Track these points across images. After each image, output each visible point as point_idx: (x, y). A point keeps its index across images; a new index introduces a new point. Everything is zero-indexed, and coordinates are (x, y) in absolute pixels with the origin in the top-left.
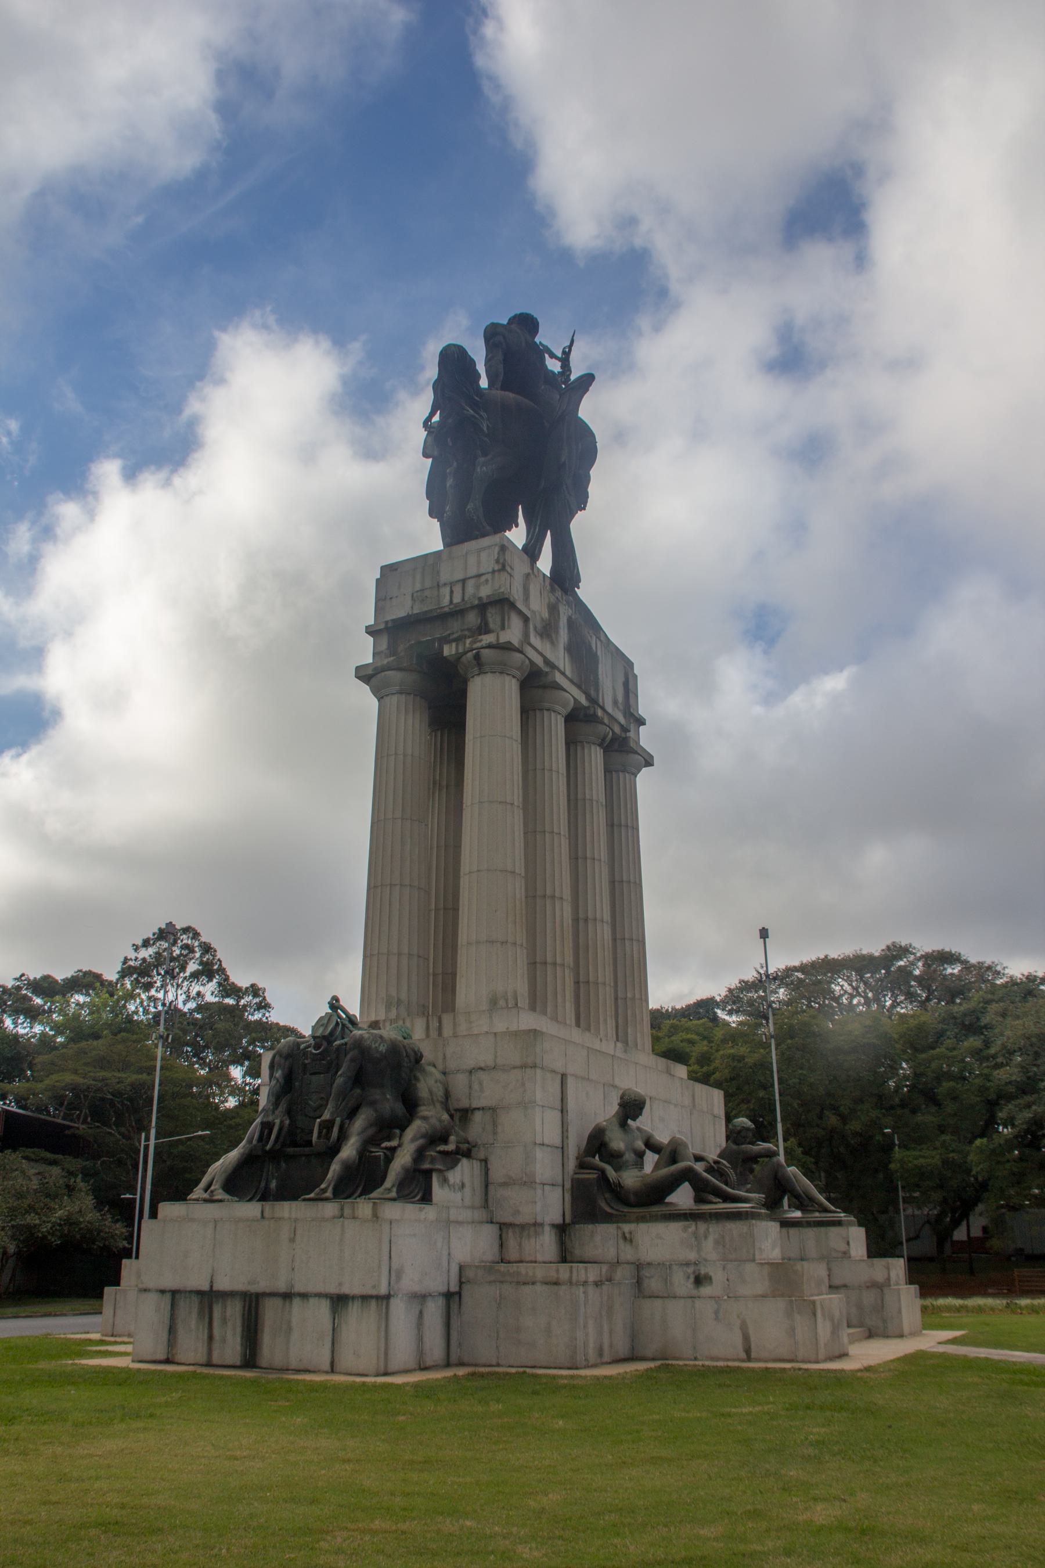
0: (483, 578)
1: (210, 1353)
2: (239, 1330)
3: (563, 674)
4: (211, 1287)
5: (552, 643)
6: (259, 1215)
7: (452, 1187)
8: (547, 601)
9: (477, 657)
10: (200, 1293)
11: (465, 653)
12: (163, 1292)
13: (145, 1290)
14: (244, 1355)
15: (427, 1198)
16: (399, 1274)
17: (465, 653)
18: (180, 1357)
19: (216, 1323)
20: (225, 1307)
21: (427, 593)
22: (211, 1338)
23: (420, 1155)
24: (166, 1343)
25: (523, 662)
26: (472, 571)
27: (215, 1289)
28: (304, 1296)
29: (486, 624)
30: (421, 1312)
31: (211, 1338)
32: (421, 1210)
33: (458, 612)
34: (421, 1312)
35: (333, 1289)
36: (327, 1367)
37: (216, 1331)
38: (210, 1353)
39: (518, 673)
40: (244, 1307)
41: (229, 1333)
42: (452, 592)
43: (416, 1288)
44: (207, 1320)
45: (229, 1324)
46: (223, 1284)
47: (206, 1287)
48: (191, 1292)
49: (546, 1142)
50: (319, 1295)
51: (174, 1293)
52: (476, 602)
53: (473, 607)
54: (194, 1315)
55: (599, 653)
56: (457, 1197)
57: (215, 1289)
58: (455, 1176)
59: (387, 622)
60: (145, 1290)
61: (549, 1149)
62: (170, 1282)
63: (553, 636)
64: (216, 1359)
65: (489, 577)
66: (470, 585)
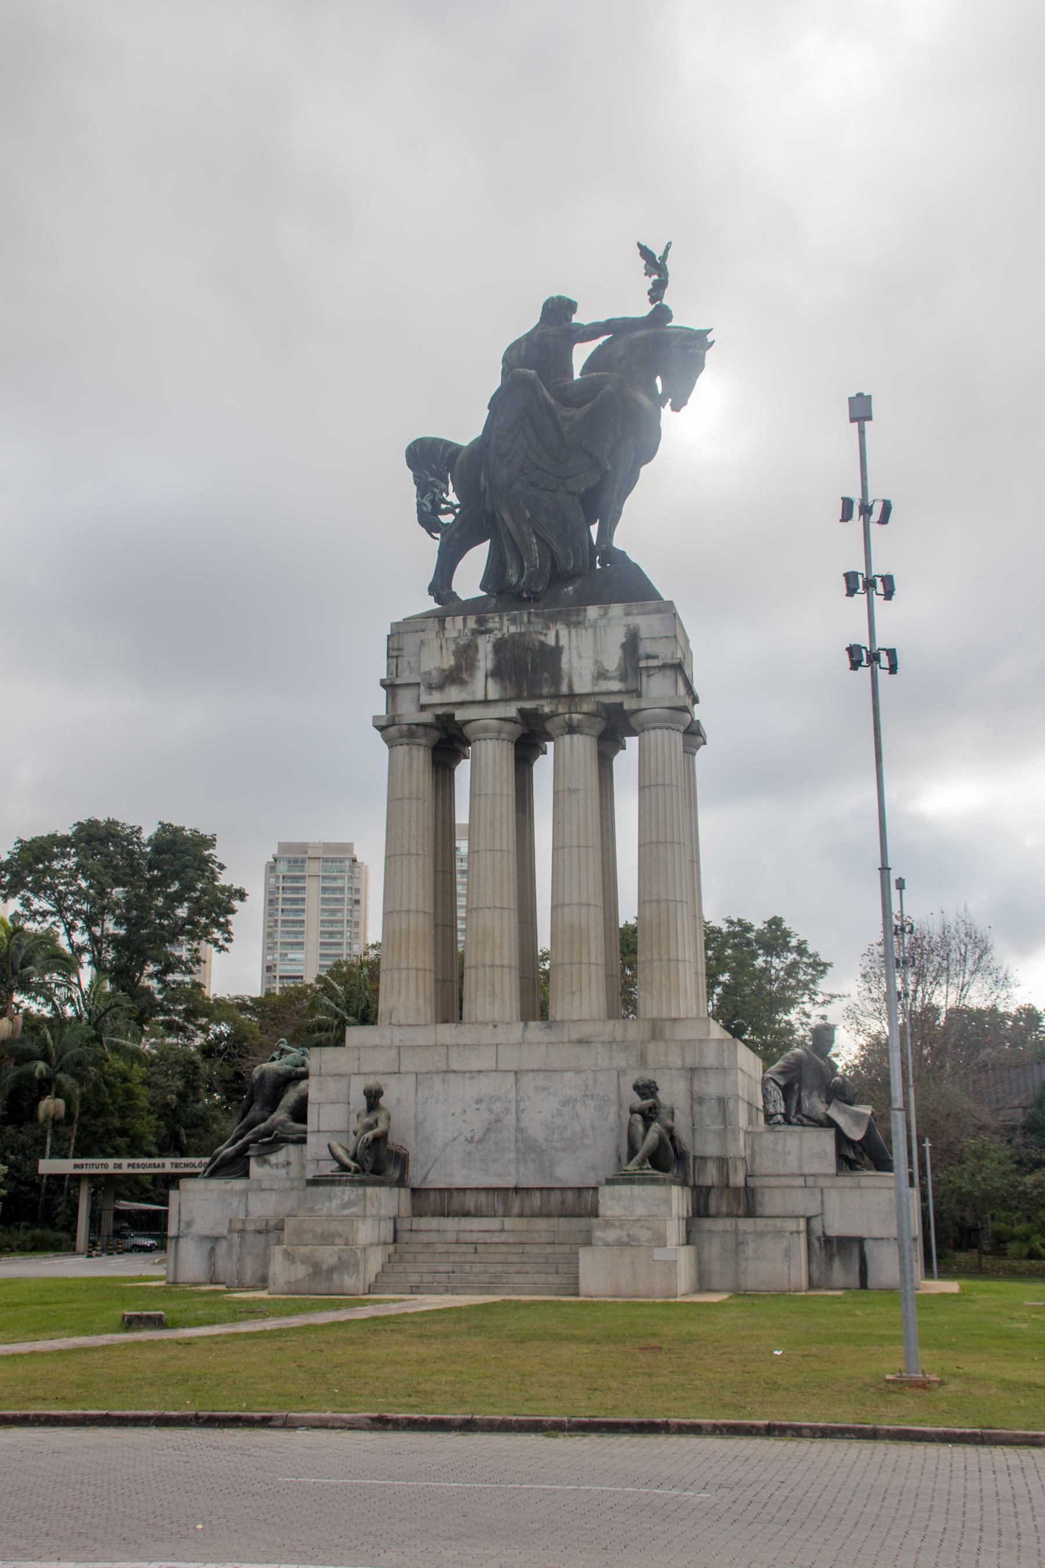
3: (486, 702)
5: (461, 682)
7: (277, 1166)
8: (452, 647)
15: (246, 1174)
16: (189, 1224)
23: (246, 1147)
25: (400, 731)
30: (213, 1249)
32: (227, 1183)
34: (213, 1249)
39: (405, 740)
43: (207, 1232)
49: (322, 1128)
55: (563, 642)
56: (283, 1172)
58: (278, 1158)
61: (327, 1134)
63: (465, 676)
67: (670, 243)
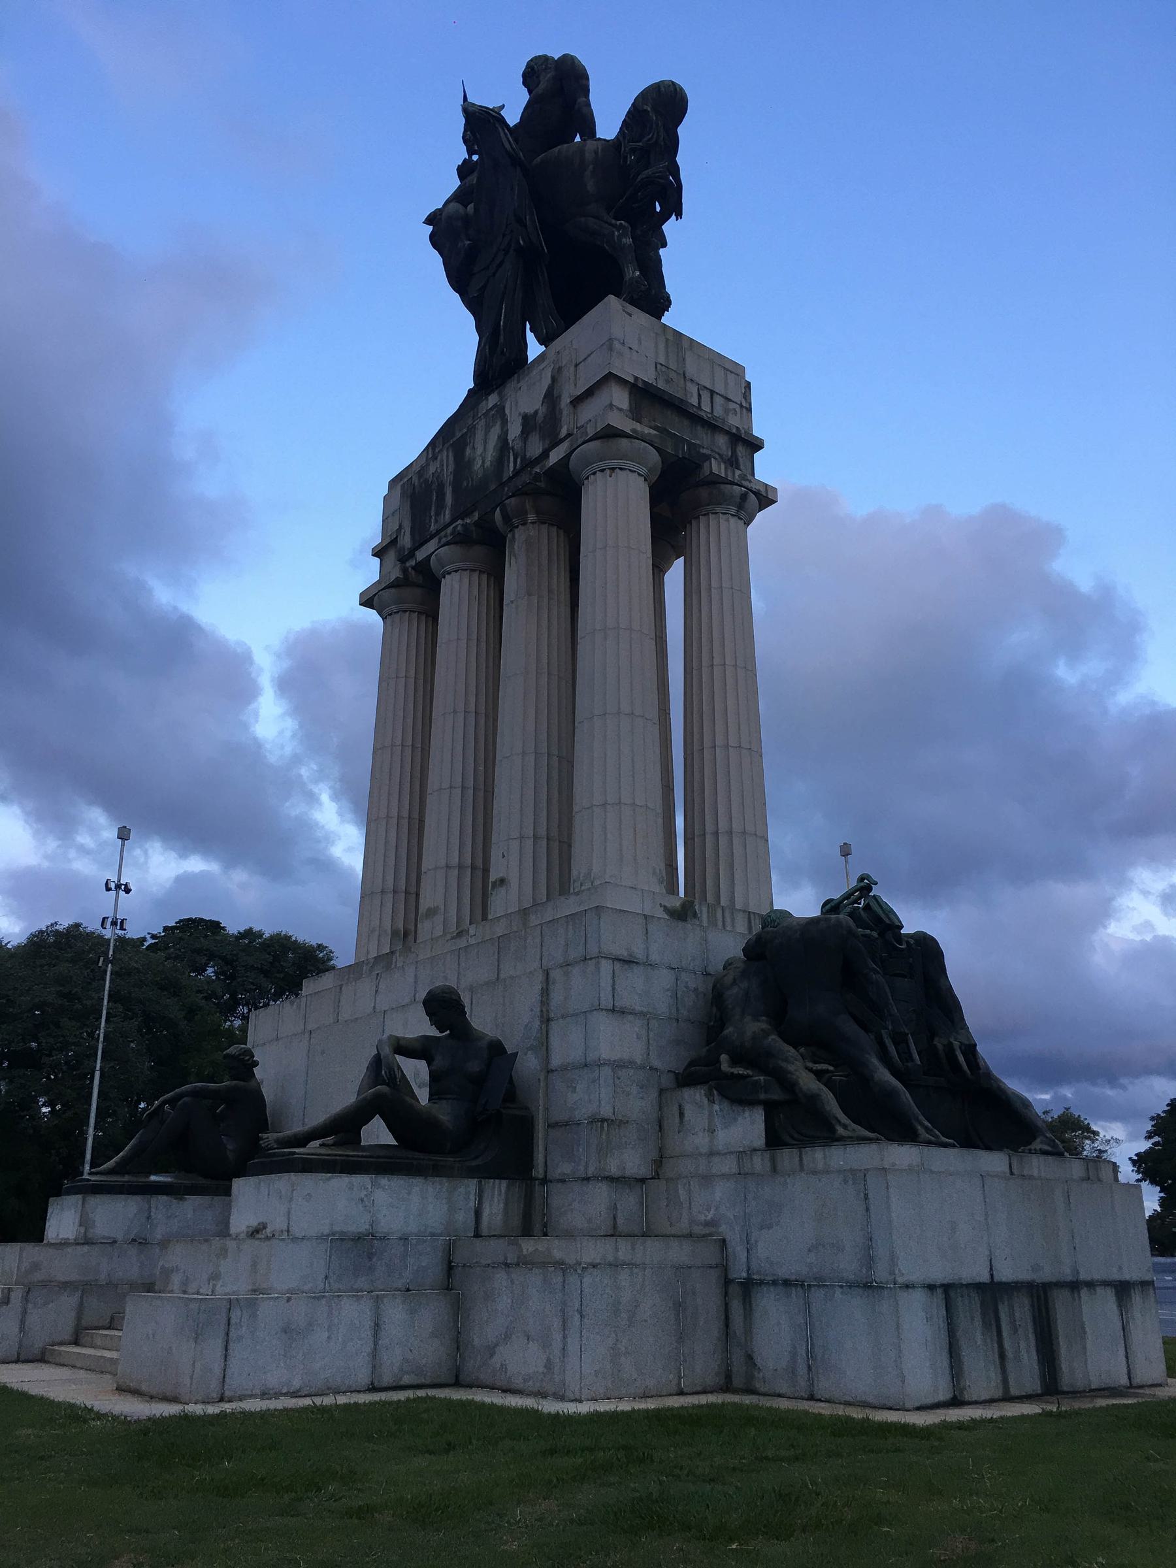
0: (732, 406)
1: (1005, 1381)
2: (1032, 1337)
4: (992, 1275)
6: (1007, 1170)
9: (744, 497)
10: (979, 1287)
11: (732, 483)
12: (931, 1287)
13: (907, 1287)
14: (1043, 1377)
17: (732, 483)
18: (973, 1394)
19: (1005, 1334)
20: (1011, 1307)
21: (673, 375)
22: (1002, 1356)
24: (947, 1371)
26: (719, 388)
27: (996, 1279)
28: (1091, 1285)
29: (737, 460)
31: (1002, 1356)
33: (712, 426)
35: (1115, 1276)
36: (1124, 1381)
37: (1007, 1344)
38: (1005, 1381)
40: (1032, 1306)
41: (1023, 1345)
42: (699, 395)
44: (994, 1327)
45: (1020, 1331)
46: (1006, 1273)
47: (985, 1278)
48: (968, 1285)
50: (1106, 1284)
51: (947, 1288)
52: (734, 431)
53: (728, 433)
54: (978, 1322)
57: (996, 1279)
59: (636, 378)
60: (907, 1287)
62: (939, 1273)
64: (1014, 1391)
65: (738, 408)
66: (718, 400)
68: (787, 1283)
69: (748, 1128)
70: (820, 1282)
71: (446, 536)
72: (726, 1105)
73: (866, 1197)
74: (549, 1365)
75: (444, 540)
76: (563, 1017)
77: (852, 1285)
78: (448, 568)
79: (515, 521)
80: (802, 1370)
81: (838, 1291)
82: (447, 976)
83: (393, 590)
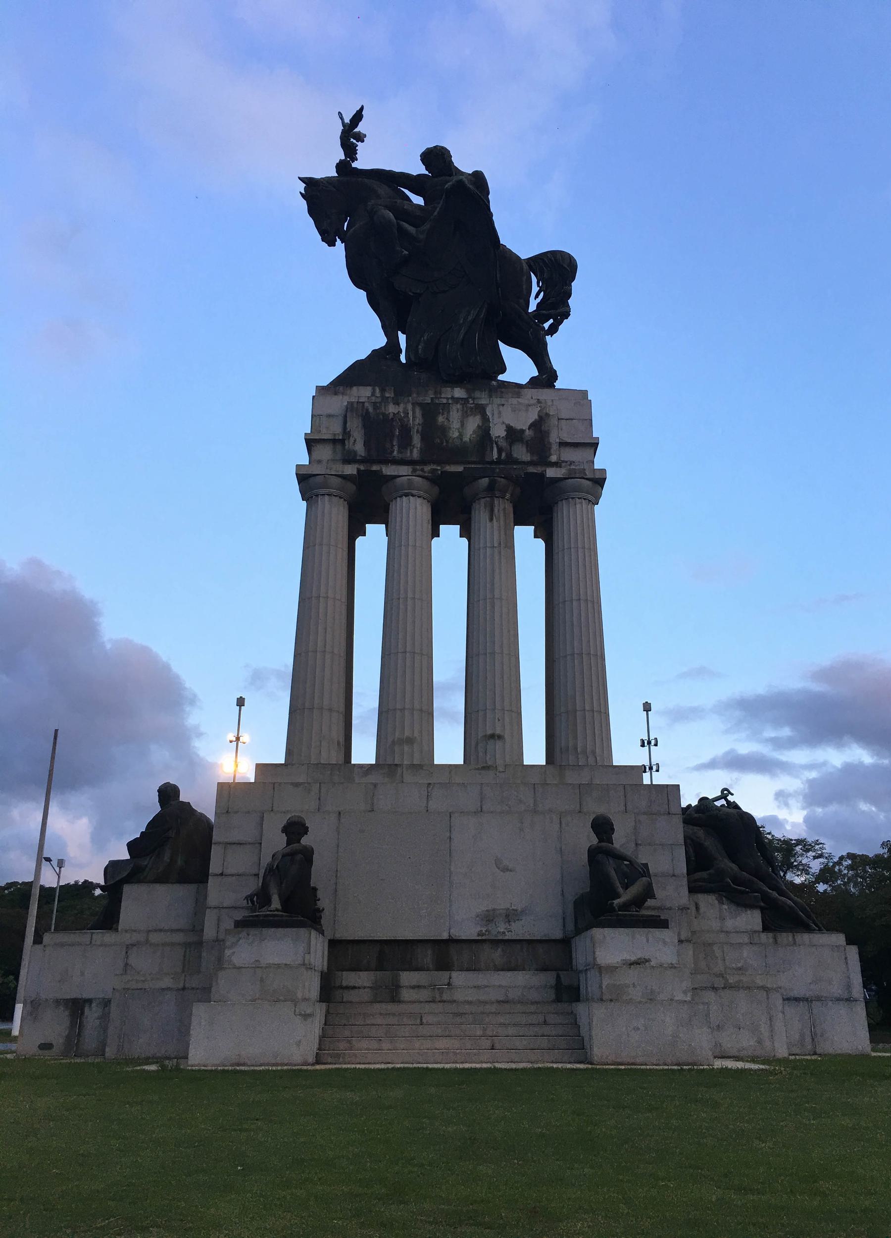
67: (339, 113)
68: (796, 999)
69: (752, 919)
70: (819, 999)
71: (422, 470)
72: (733, 907)
73: (846, 958)
74: (760, 1042)
75: (418, 473)
76: (650, 844)
77: (839, 999)
78: (414, 492)
79: (497, 494)
80: (808, 1039)
81: (830, 1003)
82: (601, 810)
83: (340, 479)
